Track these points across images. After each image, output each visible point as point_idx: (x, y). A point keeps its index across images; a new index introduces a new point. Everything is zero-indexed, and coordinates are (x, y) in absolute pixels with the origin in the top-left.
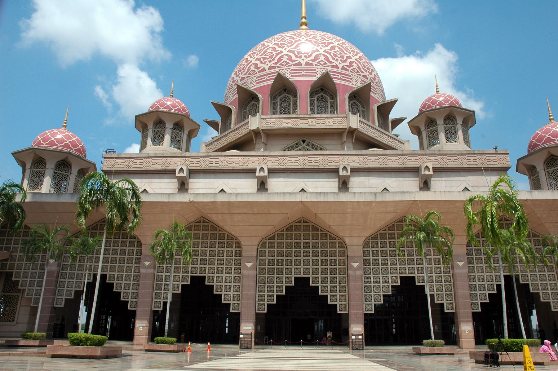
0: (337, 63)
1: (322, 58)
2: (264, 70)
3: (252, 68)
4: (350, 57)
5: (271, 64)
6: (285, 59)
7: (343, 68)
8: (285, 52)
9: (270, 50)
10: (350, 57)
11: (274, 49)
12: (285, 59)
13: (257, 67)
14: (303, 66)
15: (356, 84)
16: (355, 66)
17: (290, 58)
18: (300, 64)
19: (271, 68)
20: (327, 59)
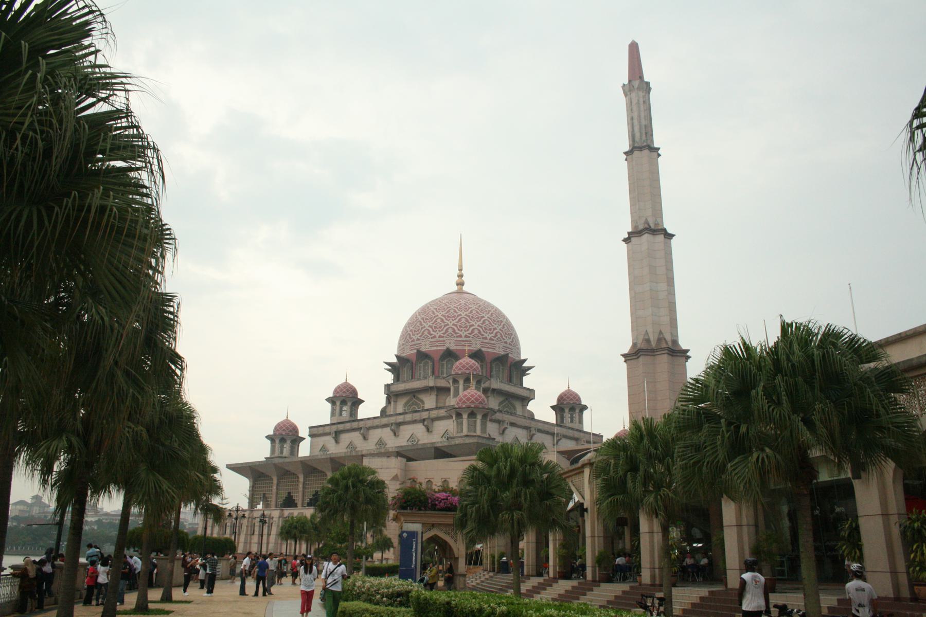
0: (486, 335)
1: (476, 332)
2: (435, 337)
3: (426, 333)
4: (495, 329)
5: (440, 333)
6: (450, 331)
7: (491, 339)
8: (451, 325)
9: (439, 321)
10: (495, 329)
11: (442, 321)
12: (450, 331)
13: (429, 333)
14: (463, 338)
15: (499, 351)
16: (499, 335)
17: (454, 331)
18: (461, 336)
19: (440, 337)
20: (480, 332)
